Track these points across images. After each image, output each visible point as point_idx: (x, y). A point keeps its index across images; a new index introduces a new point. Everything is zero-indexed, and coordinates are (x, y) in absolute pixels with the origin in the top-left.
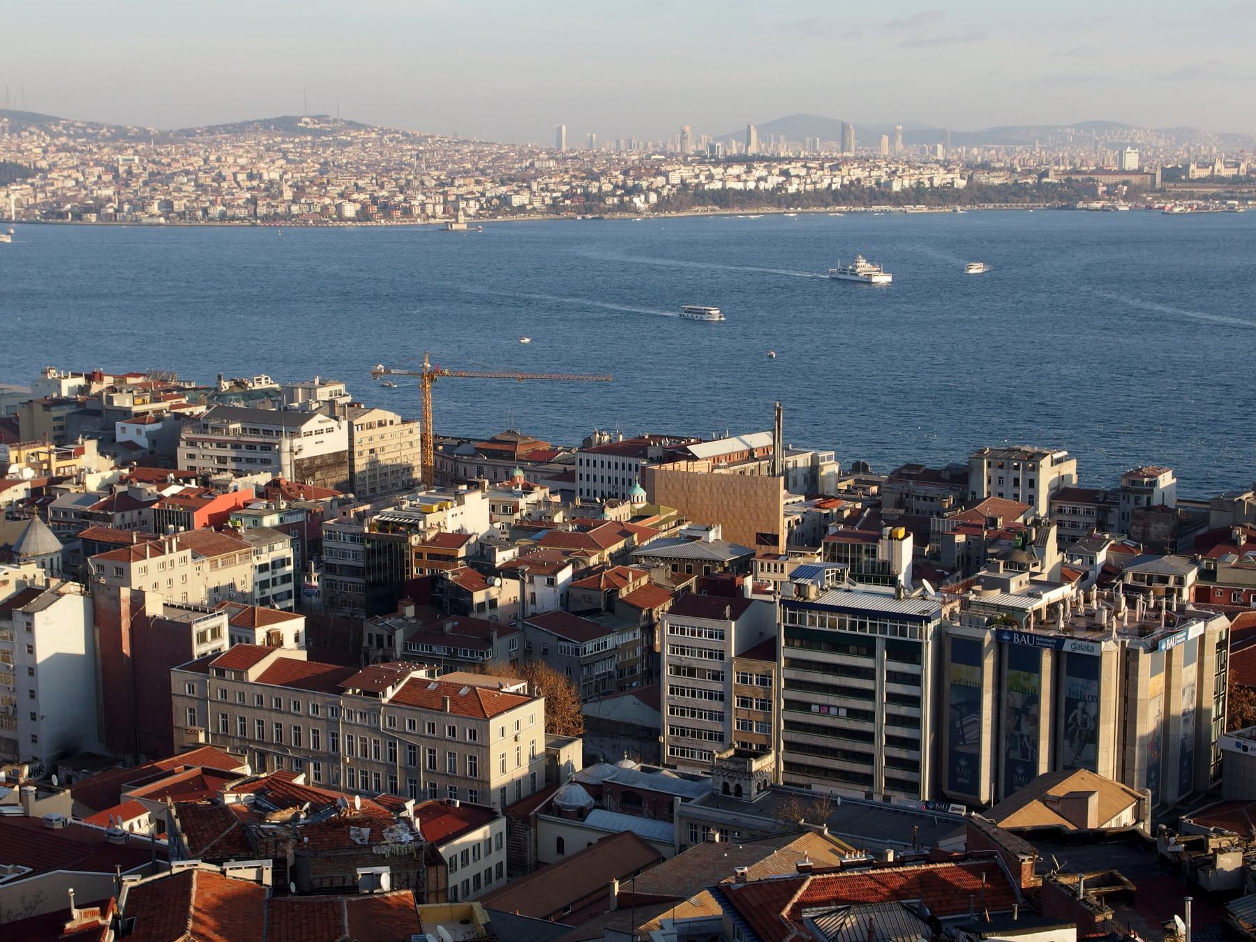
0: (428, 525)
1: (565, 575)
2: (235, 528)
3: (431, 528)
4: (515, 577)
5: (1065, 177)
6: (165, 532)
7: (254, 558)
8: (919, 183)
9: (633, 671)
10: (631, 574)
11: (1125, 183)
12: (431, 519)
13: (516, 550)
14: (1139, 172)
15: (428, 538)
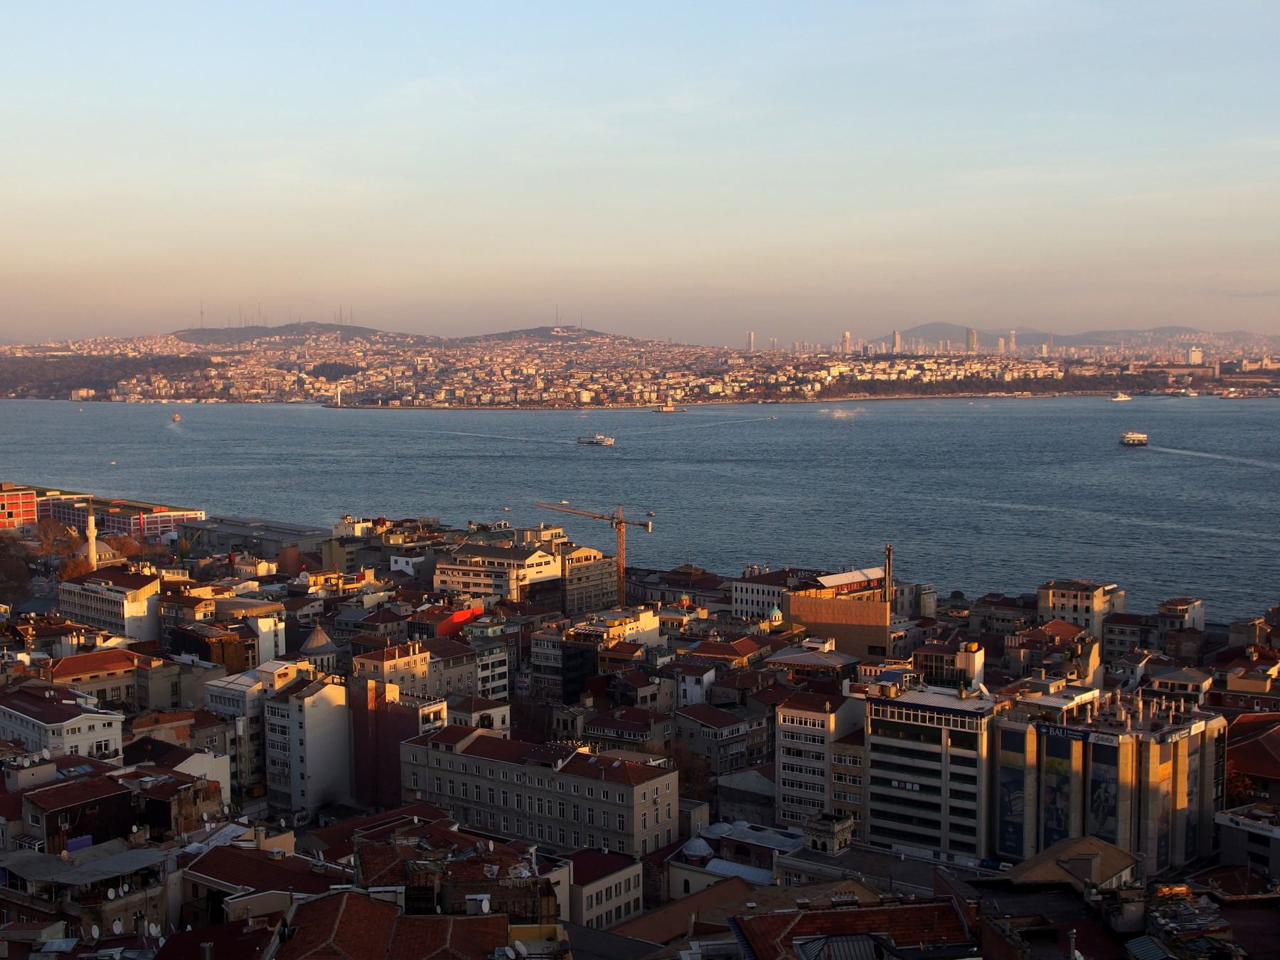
0: (611, 636)
1: (709, 676)
2: (465, 636)
3: (613, 639)
4: (671, 677)
5: (1143, 370)
6: (412, 639)
7: (478, 660)
8: (1026, 375)
9: (760, 751)
10: (760, 676)
11: (1190, 375)
12: (614, 632)
13: (674, 657)
14: (1201, 366)
15: (611, 646)
